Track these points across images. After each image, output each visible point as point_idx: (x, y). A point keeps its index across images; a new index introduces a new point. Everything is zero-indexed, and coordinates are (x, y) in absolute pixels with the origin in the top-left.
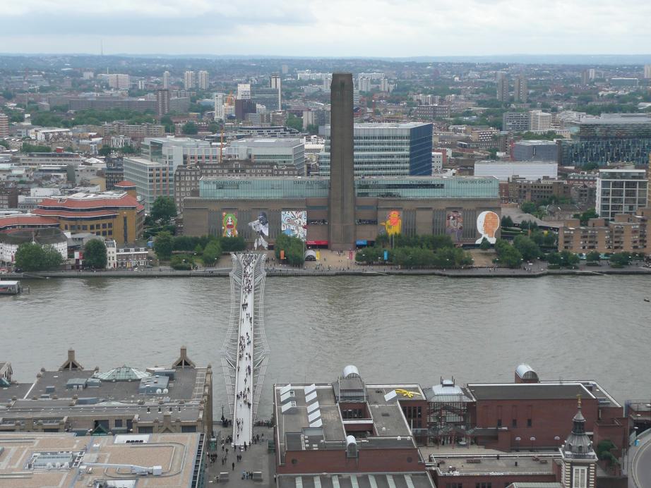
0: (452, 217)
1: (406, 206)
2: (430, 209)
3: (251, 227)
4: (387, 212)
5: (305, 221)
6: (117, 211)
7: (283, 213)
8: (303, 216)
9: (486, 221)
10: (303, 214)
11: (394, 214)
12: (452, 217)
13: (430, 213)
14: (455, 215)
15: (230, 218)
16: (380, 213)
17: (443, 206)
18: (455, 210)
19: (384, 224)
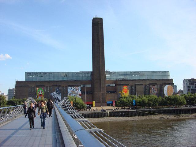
0: (152, 88)
1: (131, 83)
2: (142, 84)
3: (52, 96)
4: (122, 86)
5: (80, 92)
7: (69, 87)
8: (80, 89)
9: (168, 90)
10: (79, 88)
11: (125, 88)
12: (152, 88)
14: (154, 87)
15: (40, 91)
16: (118, 87)
17: (148, 83)
18: (154, 85)
19: (120, 92)
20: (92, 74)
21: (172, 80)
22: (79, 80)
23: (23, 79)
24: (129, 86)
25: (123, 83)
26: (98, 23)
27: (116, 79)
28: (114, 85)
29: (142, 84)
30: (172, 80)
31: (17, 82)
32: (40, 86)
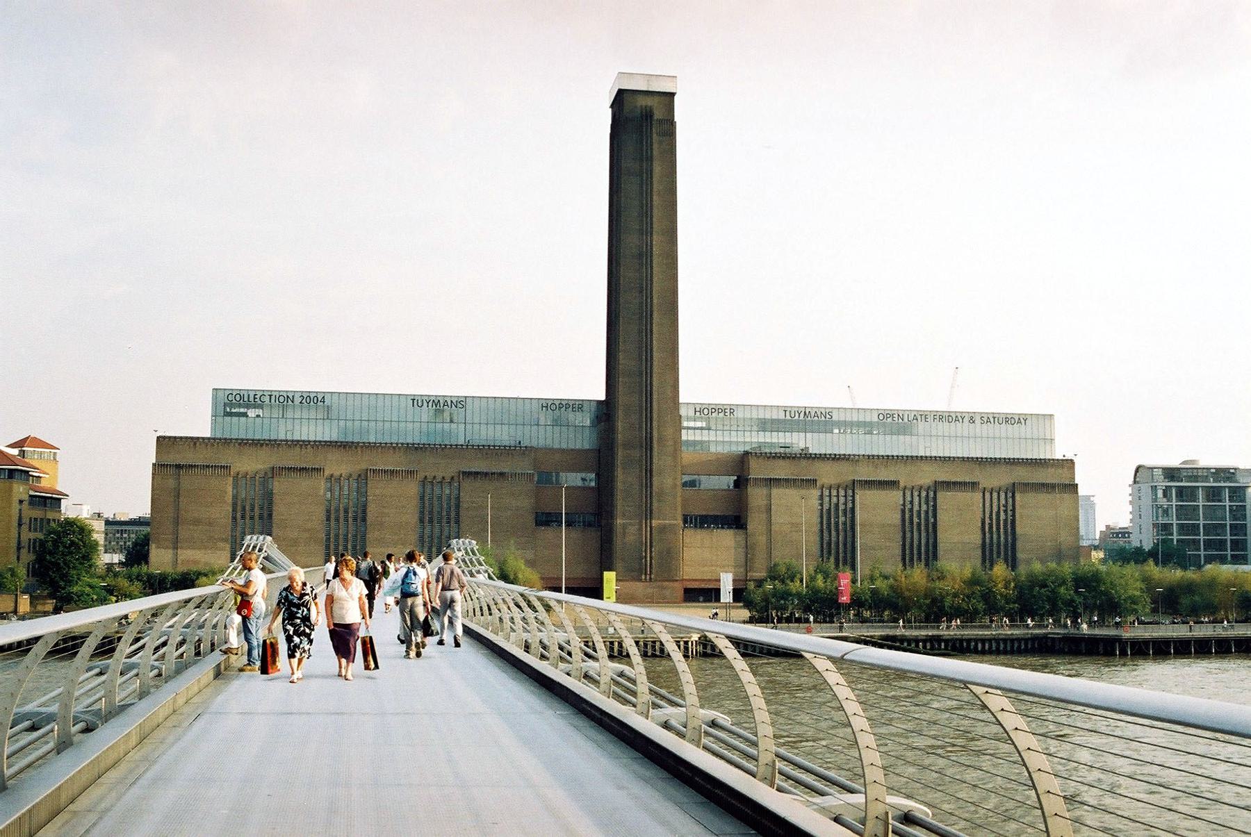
1: (828, 475)
2: (892, 484)
13: (895, 497)
16: (756, 495)
17: (927, 476)
20: (605, 412)
21: (1069, 464)
22: (525, 443)
23: (202, 427)
24: (815, 493)
25: (781, 470)
26: (648, 115)
27: (741, 449)
28: (728, 481)
29: (892, 484)
30: (1069, 464)
31: (164, 443)
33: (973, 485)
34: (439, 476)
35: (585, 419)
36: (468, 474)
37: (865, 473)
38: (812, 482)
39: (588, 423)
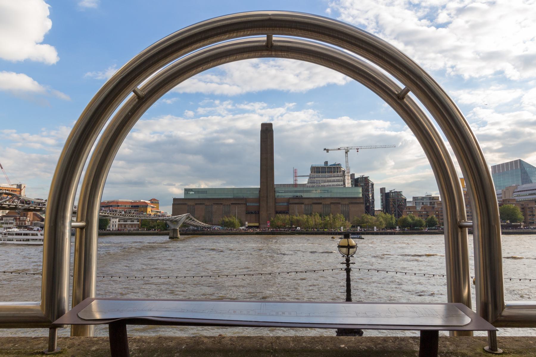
1: (306, 202)
2: (321, 203)
6: (138, 208)
13: (321, 206)
16: (291, 206)
17: (328, 202)
20: (260, 190)
24: (303, 206)
27: (288, 197)
28: (286, 204)
29: (321, 203)
31: (175, 200)
32: (200, 204)
33: (339, 203)
34: (227, 204)
35: (257, 192)
36: (232, 204)
37: (315, 201)
38: (303, 203)
39: (257, 192)
